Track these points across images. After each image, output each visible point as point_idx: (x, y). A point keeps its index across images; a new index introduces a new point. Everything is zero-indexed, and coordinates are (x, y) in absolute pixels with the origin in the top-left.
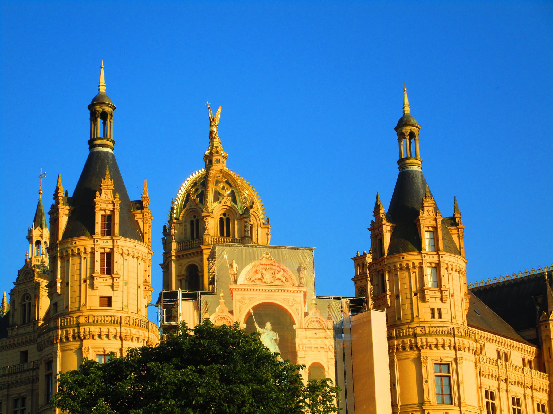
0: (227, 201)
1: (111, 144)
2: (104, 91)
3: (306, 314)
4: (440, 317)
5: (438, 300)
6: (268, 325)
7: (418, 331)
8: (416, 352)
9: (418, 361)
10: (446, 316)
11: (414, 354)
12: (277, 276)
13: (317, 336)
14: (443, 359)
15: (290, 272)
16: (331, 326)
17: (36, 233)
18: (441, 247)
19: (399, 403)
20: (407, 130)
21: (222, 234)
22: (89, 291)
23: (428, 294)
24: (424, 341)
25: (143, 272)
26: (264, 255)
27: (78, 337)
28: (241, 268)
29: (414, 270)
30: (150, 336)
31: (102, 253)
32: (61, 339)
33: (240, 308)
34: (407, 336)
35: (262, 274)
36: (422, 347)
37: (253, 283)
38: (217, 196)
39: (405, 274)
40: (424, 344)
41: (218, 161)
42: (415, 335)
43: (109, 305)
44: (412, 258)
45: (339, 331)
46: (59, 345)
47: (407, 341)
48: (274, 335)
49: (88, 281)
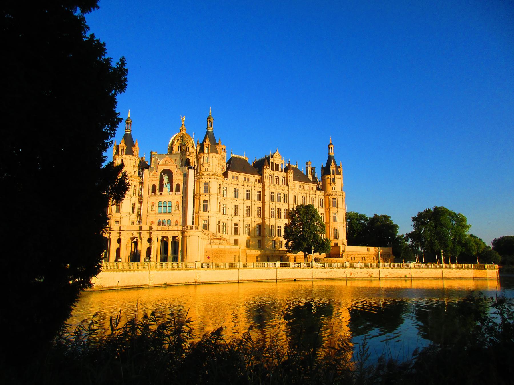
0: (180, 142)
1: (130, 131)
3: (176, 171)
6: (166, 174)
12: (170, 162)
15: (173, 160)
16: (183, 173)
18: (209, 151)
19: (195, 193)
23: (204, 165)
28: (160, 160)
34: (197, 176)
38: (178, 140)
44: (201, 155)
48: (167, 177)
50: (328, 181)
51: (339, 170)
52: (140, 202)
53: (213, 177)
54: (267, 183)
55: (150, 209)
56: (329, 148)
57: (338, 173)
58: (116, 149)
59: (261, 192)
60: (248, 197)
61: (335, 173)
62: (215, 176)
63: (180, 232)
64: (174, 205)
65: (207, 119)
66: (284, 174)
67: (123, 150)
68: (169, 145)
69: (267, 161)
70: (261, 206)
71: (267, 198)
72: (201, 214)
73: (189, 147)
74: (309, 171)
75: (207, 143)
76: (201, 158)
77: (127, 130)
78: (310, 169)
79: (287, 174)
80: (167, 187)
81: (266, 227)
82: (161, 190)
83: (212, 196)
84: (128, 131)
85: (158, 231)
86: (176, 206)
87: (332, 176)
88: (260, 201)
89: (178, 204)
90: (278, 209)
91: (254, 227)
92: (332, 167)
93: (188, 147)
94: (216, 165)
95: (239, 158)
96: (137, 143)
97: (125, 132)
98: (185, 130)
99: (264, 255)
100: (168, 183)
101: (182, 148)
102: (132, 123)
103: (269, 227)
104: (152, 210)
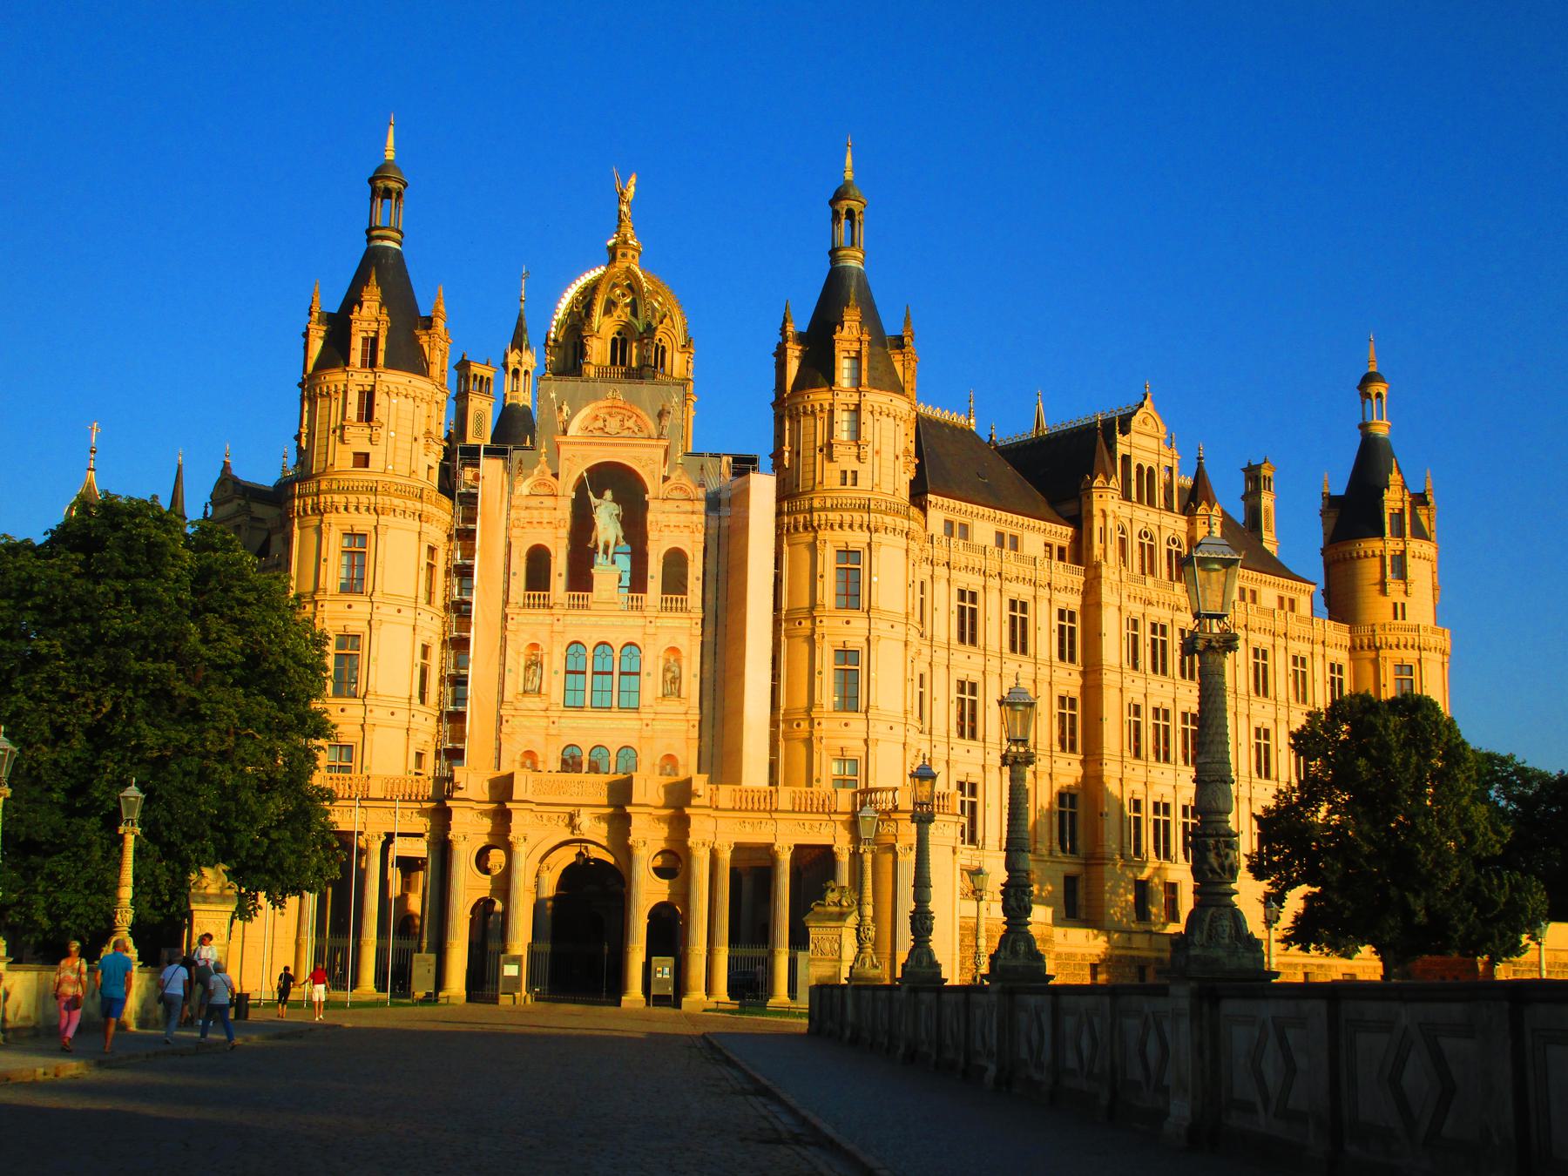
0: (622, 314)
1: (398, 236)
2: (392, 158)
3: (666, 479)
4: (855, 484)
5: (854, 459)
6: (608, 494)
7: (816, 504)
8: (812, 534)
9: (813, 548)
10: (864, 482)
11: (809, 537)
12: (630, 423)
13: (679, 510)
14: (850, 545)
15: (647, 418)
16: (701, 493)
17: (513, 358)
18: (864, 381)
19: (785, 605)
20: (844, 206)
21: (613, 361)
22: (339, 446)
23: (837, 450)
24: (823, 517)
25: (424, 420)
26: (610, 393)
27: (316, 509)
28: (574, 412)
29: (822, 415)
30: (425, 509)
31: (360, 392)
32: (298, 512)
33: (569, 470)
34: (801, 512)
35: (605, 421)
36: (819, 526)
37: (590, 434)
38: (610, 306)
39: (810, 420)
40: (823, 522)
41: (624, 255)
42: (811, 510)
43: (367, 465)
44: (819, 397)
45: (714, 503)
46: (296, 520)
47: (801, 518)
48: (615, 509)
49: (338, 432)
50: (1370, 571)
51: (1422, 513)
52: (459, 645)
53: (888, 520)
54: (1111, 570)
55: (514, 683)
56: (1369, 396)
57: (1419, 532)
58: (322, 334)
59: (1078, 618)
60: (1019, 640)
61: (1408, 528)
62: (898, 520)
63: (842, 822)
64: (652, 663)
65: (832, 203)
66: (1175, 525)
67: (375, 341)
68: (553, 329)
69: (1104, 448)
70: (1075, 692)
71: (1112, 650)
72: (823, 722)
73: (668, 347)
74: (1267, 511)
75: (849, 336)
76: (813, 412)
77: (378, 228)
78: (1267, 500)
79: (1191, 524)
80: (613, 562)
81: (1106, 809)
82: (580, 579)
83: (880, 627)
84: (388, 238)
85: (717, 808)
86: (666, 670)
87: (1391, 545)
88: (1071, 666)
89: (678, 660)
90: (1156, 710)
91: (1046, 806)
92: (1393, 499)
93: (663, 347)
94: (897, 457)
95: (945, 425)
96: (442, 308)
97: (370, 239)
98: (636, 254)
99: (1125, 957)
100: (623, 543)
101: (635, 352)
102: (405, 193)
103: (1122, 806)
104: (529, 687)
